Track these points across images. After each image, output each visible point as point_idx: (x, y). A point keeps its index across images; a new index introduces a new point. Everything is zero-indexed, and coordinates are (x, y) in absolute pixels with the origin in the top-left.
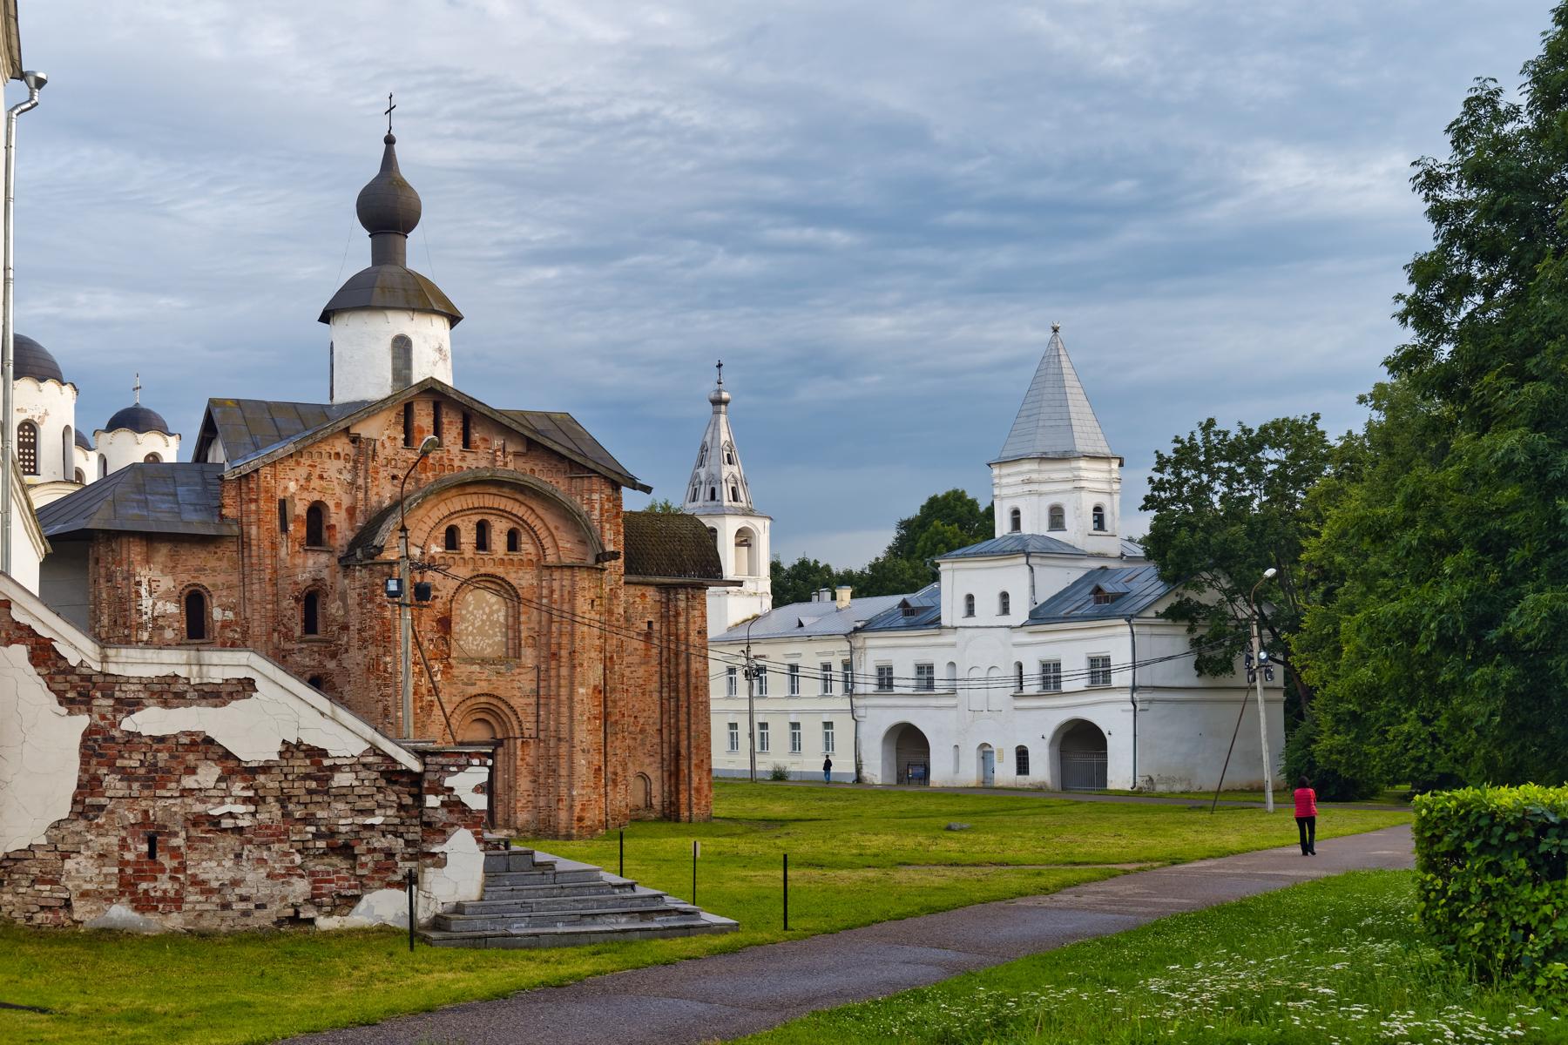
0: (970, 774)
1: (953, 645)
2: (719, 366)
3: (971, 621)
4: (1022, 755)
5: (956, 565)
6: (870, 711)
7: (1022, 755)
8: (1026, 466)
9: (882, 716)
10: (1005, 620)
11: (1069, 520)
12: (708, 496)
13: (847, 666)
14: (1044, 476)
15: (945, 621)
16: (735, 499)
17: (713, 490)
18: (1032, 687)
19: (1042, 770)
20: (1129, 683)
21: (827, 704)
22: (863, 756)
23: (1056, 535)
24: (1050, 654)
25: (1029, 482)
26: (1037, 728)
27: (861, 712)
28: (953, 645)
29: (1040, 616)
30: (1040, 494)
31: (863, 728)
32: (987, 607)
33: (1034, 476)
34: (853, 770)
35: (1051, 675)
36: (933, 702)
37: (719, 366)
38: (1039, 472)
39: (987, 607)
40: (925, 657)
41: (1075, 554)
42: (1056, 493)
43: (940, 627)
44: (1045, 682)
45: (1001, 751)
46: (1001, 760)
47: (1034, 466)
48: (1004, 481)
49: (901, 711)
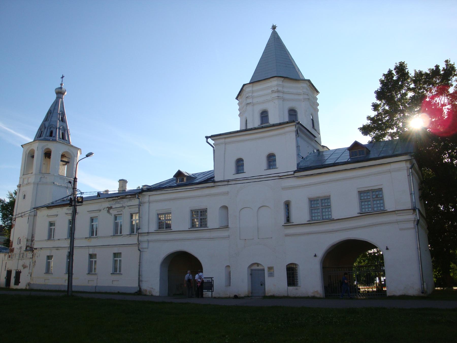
0: (241, 285)
2: (63, 77)
4: (292, 273)
7: (292, 273)
12: (48, 134)
14: (285, 90)
15: (216, 179)
17: (51, 133)
20: (409, 206)
21: (119, 240)
25: (278, 91)
30: (284, 100)
33: (280, 89)
35: (320, 208)
37: (63, 77)
40: (198, 204)
43: (214, 182)
46: (271, 275)
48: (255, 94)
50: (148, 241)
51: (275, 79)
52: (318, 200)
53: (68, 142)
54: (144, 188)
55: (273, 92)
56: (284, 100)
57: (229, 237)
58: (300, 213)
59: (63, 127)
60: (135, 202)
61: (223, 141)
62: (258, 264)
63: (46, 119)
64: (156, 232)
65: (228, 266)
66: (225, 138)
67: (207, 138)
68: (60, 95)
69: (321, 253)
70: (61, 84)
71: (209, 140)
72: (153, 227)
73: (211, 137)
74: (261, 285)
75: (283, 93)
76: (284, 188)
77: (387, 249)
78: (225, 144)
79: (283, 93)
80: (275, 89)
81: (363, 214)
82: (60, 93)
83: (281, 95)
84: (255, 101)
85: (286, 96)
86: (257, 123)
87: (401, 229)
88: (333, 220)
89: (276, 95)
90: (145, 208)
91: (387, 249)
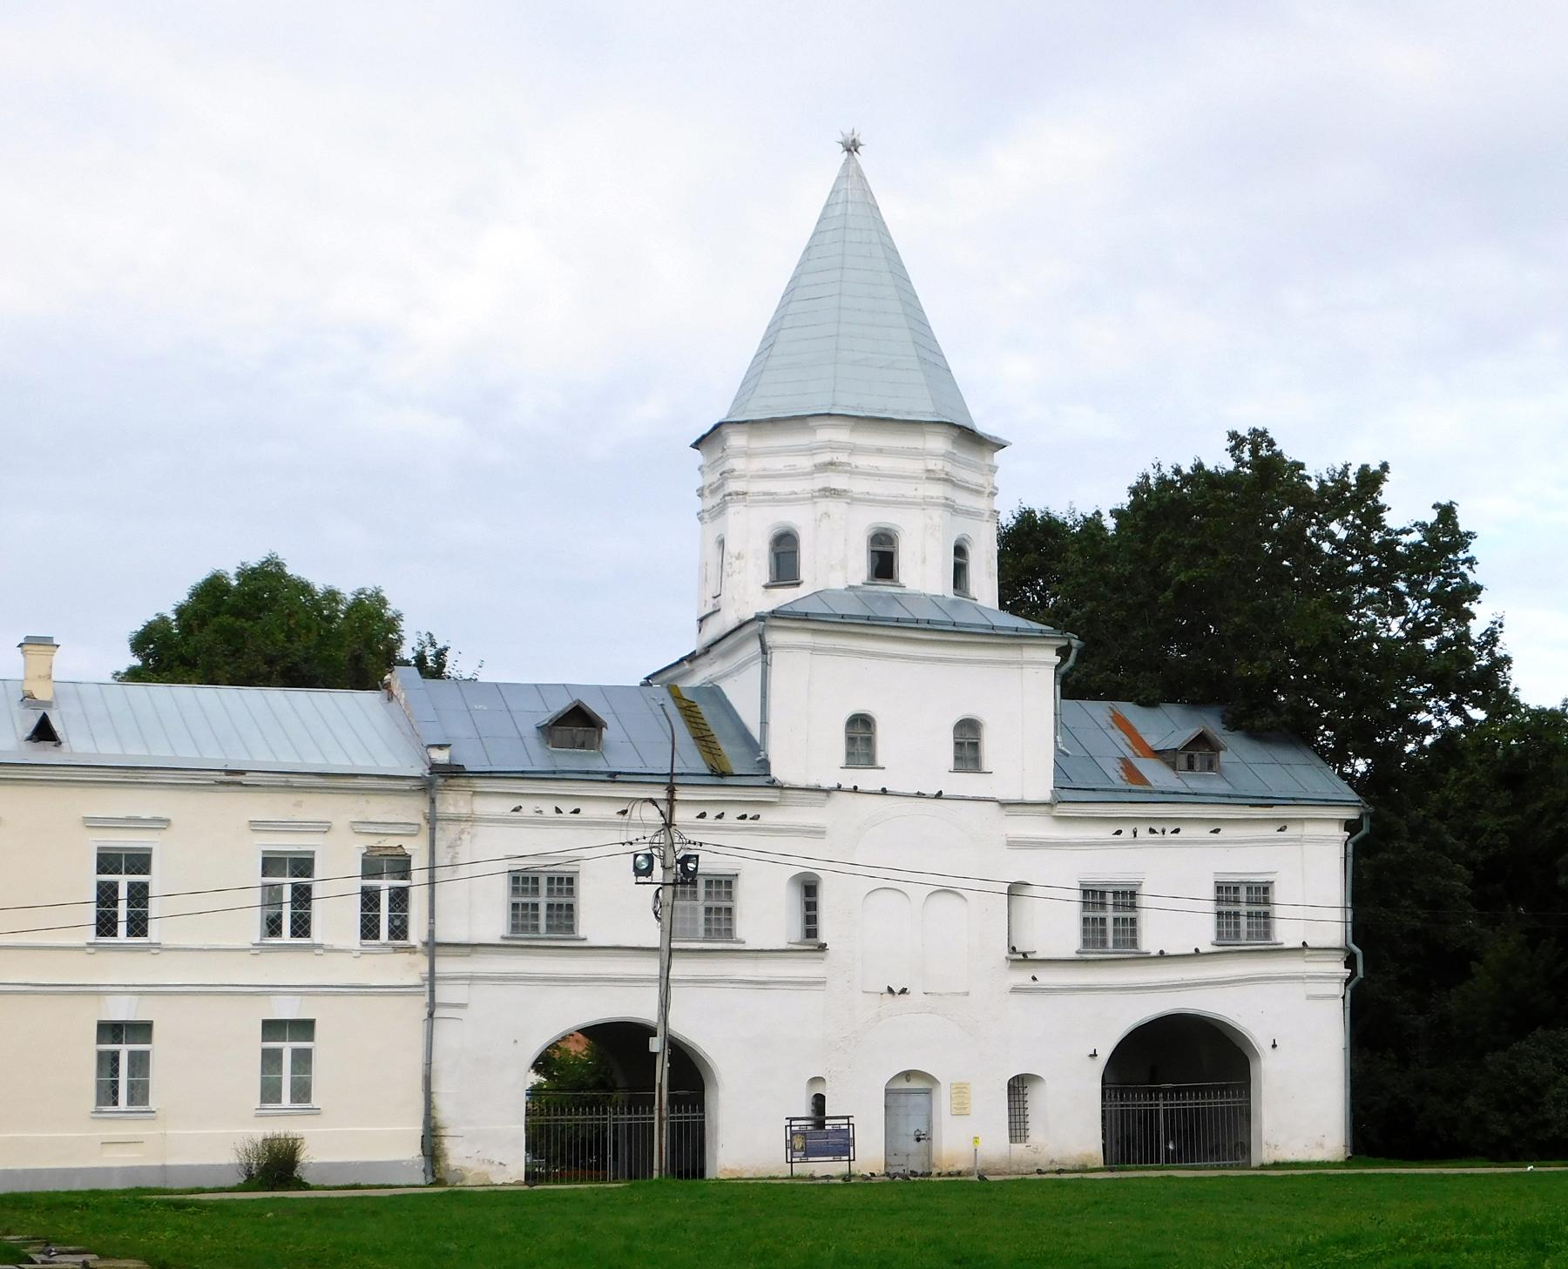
1: (818, 832)
10: (968, 783)
19: (1071, 1128)
22: (446, 1111)
24: (1112, 864)
25: (948, 480)
26: (1072, 1039)
27: (444, 993)
28: (818, 832)
32: (914, 749)
34: (411, 1152)
35: (1110, 917)
39: (914, 749)
44: (1092, 930)
45: (961, 1090)
46: (961, 1110)
49: (618, 991)
50: (472, 979)
51: (938, 429)
52: (1103, 893)
55: (931, 476)
56: (950, 507)
58: (1057, 927)
62: (908, 1075)
66: (814, 631)
72: (493, 922)
74: (918, 1140)
76: (1013, 844)
77: (1274, 1046)
80: (936, 465)
84: (858, 486)
86: (833, 565)
87: (1309, 997)
88: (1146, 958)
89: (937, 491)
91: (1274, 1046)
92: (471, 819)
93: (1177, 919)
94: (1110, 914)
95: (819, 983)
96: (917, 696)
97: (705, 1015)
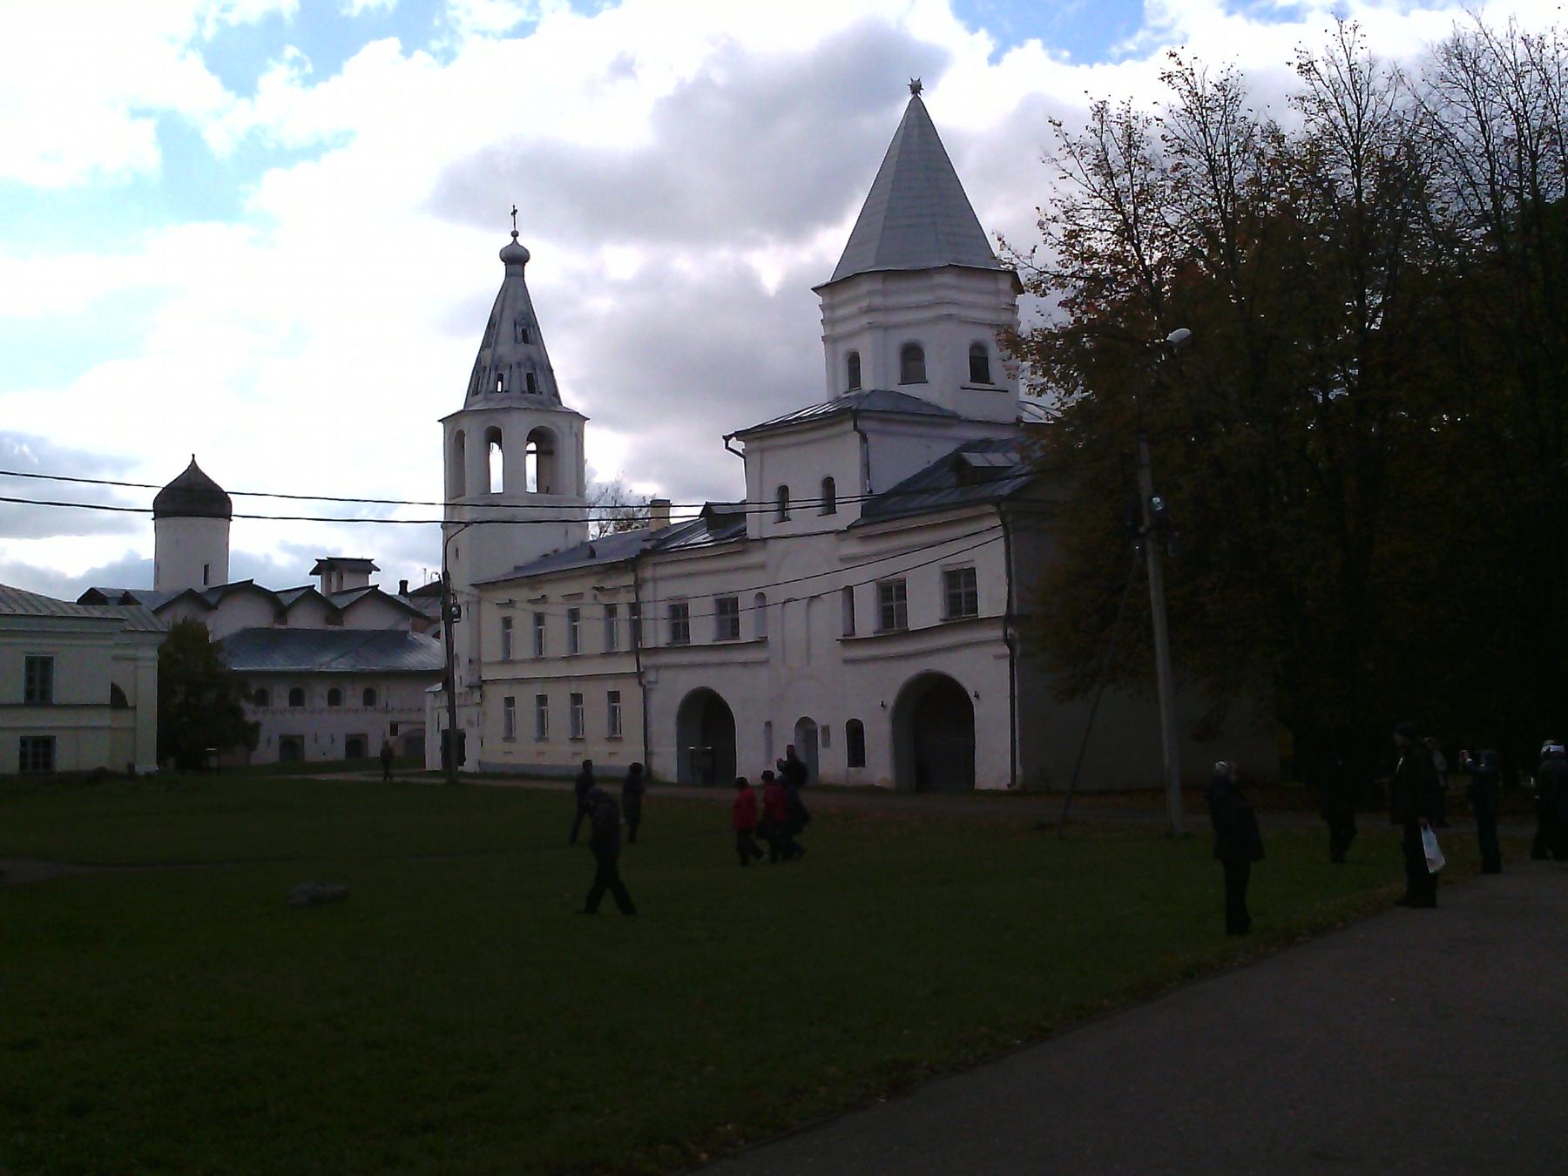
1: (762, 567)
2: (514, 213)
3: (786, 529)
5: (768, 443)
6: (665, 675)
8: (865, 286)
9: (674, 687)
11: (934, 366)
13: (635, 608)
14: (892, 301)
16: (531, 389)
18: (867, 622)
20: (1002, 611)
23: (912, 390)
25: (870, 310)
27: (651, 676)
28: (762, 567)
29: (881, 510)
30: (886, 328)
31: (656, 698)
33: (878, 301)
36: (738, 656)
37: (514, 213)
38: (885, 293)
41: (940, 418)
42: (908, 325)
45: (826, 730)
46: (827, 743)
47: (877, 285)
48: (840, 312)
50: (657, 668)
53: (545, 397)
54: (648, 546)
56: (886, 328)
57: (765, 662)
59: (529, 359)
60: (628, 580)
61: (755, 445)
63: (485, 345)
64: (669, 649)
65: (768, 724)
67: (727, 438)
68: (517, 267)
69: (890, 701)
70: (515, 234)
71: (733, 443)
73: (738, 435)
75: (887, 310)
77: (977, 696)
78: (762, 451)
79: (887, 310)
80: (864, 303)
81: (946, 626)
82: (515, 259)
83: (880, 318)
85: (896, 318)
89: (865, 320)
90: (647, 593)
92: (655, 580)
93: (926, 607)
94: (894, 604)
95: (765, 662)
96: (802, 470)
97: (734, 687)
